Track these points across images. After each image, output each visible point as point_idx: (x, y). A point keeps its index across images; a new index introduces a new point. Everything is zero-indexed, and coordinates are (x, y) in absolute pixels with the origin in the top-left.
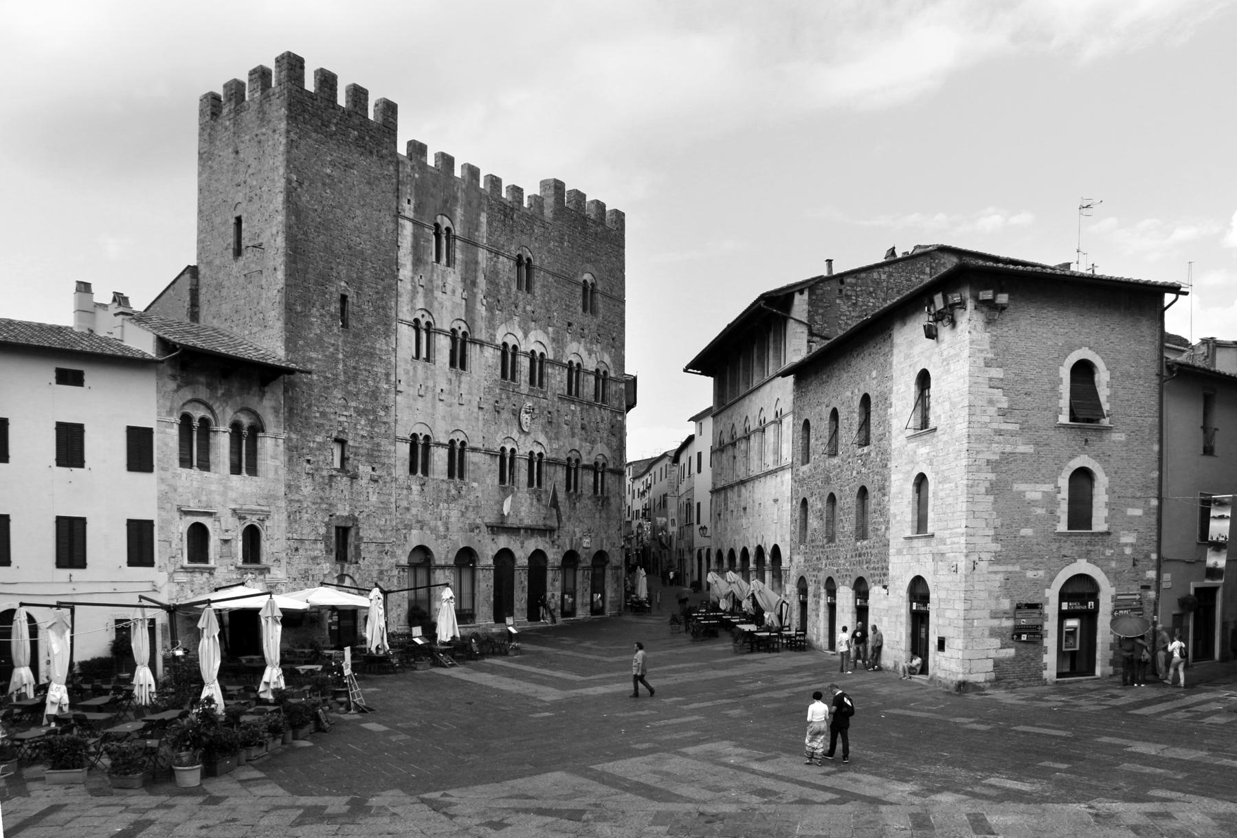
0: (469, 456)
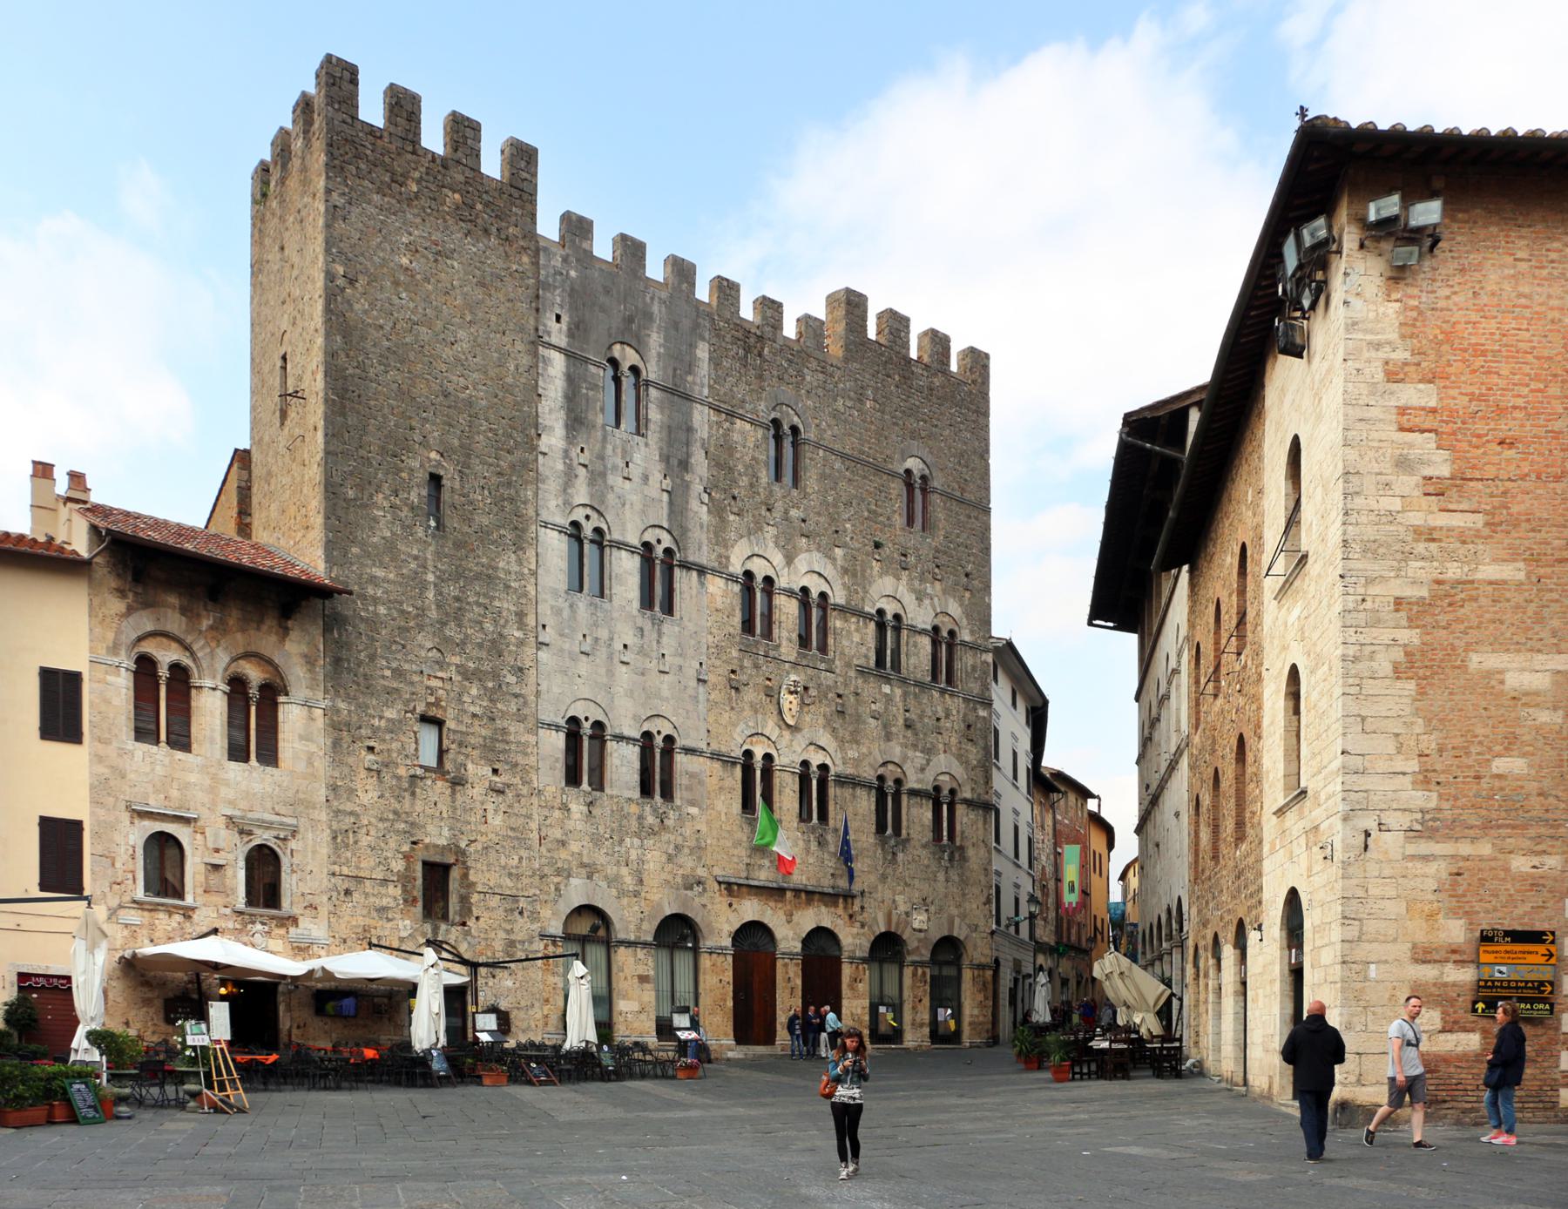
0: (680, 759)
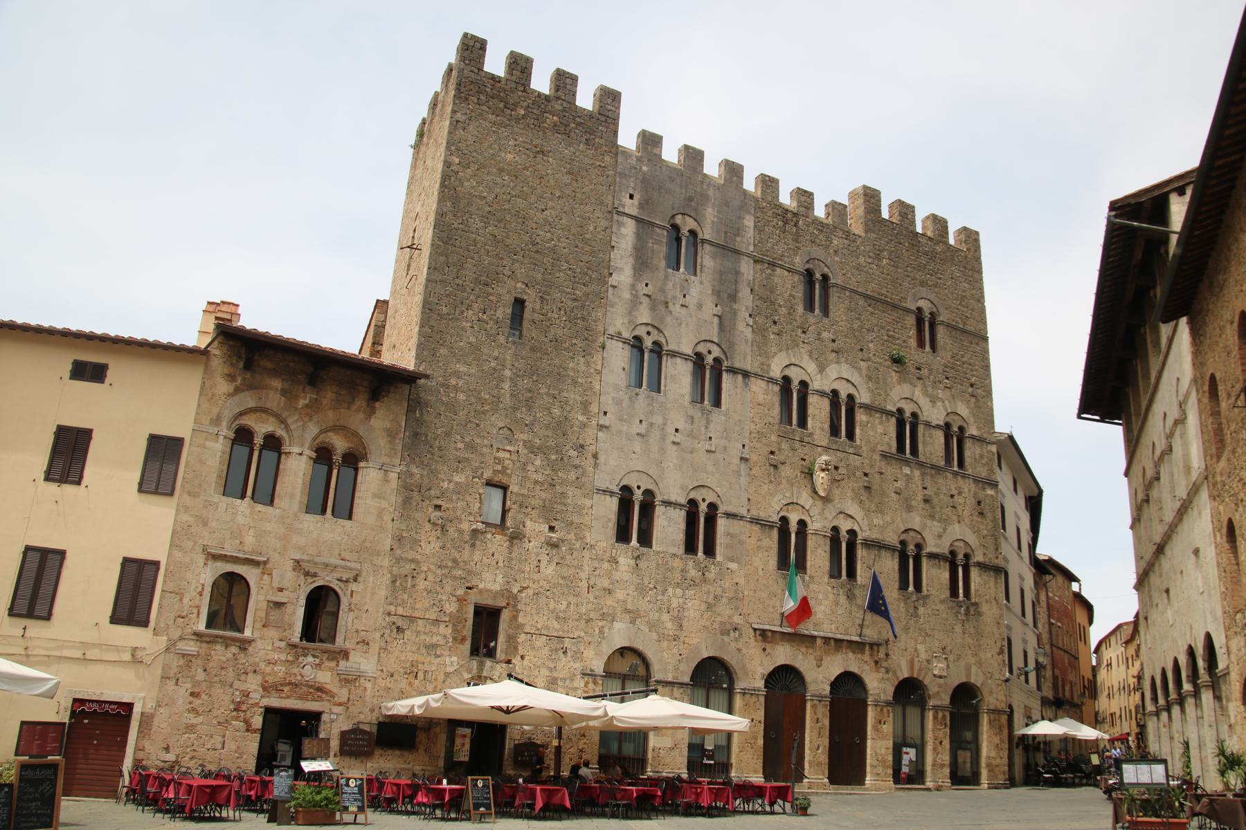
0: (722, 524)
